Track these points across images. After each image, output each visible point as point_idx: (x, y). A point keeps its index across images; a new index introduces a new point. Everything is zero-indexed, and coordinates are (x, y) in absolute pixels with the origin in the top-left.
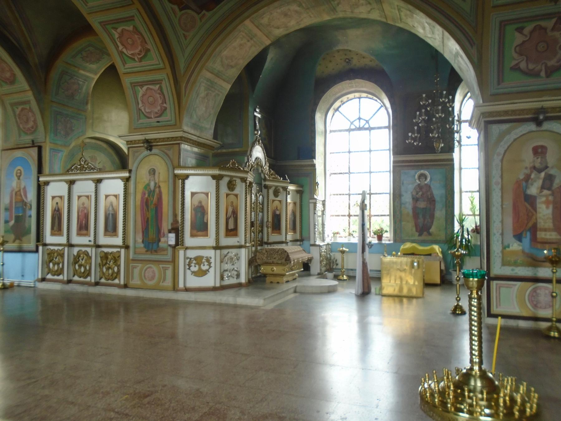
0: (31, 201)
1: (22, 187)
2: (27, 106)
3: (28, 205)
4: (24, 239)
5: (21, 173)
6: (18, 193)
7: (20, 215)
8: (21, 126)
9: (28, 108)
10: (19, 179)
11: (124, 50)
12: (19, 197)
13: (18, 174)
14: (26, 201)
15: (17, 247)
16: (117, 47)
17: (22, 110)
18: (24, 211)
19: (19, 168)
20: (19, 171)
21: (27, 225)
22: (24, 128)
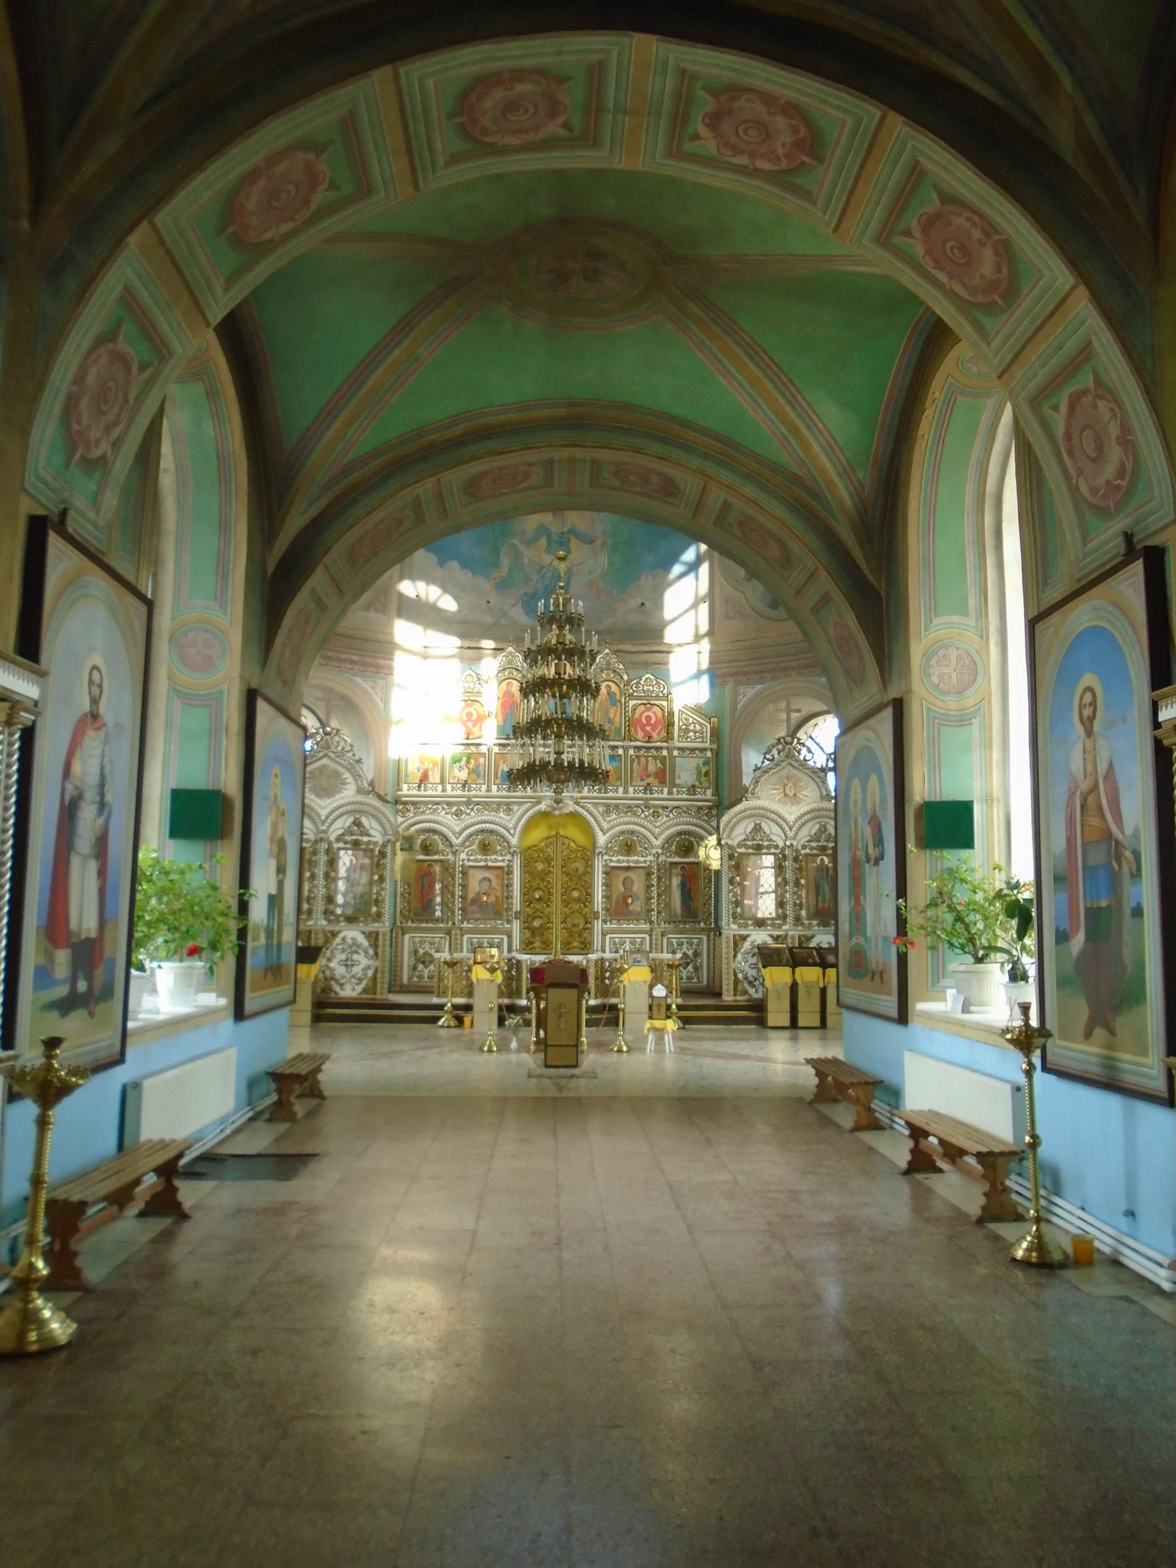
0: (1136, 834)
1: (1102, 768)
3: (1128, 854)
4: (1122, 1023)
5: (1094, 704)
6: (1091, 799)
10: (1089, 733)
12: (1094, 821)
13: (1087, 712)
14: (1120, 837)
15: (1095, 1060)
18: (1115, 885)
19: (1088, 679)
20: (1088, 698)
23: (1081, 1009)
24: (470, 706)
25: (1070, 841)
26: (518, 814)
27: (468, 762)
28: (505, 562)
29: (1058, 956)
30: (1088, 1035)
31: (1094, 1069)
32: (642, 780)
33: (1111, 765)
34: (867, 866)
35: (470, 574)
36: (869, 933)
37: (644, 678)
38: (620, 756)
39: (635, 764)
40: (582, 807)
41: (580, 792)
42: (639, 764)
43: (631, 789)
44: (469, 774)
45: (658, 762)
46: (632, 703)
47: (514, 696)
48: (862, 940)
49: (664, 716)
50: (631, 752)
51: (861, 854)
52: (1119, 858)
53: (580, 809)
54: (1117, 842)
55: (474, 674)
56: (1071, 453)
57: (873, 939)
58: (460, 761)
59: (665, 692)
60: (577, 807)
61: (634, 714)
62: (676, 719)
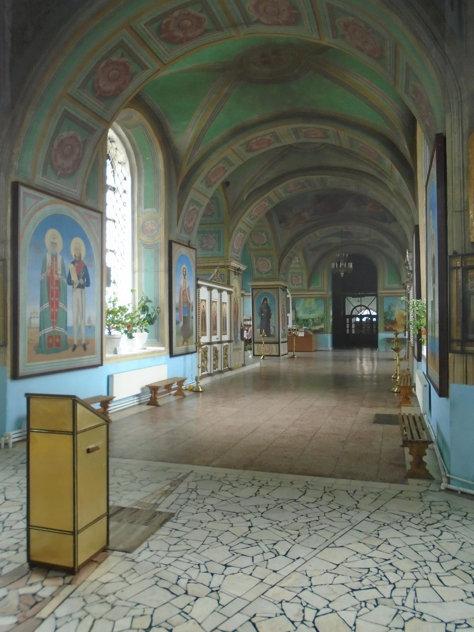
0: (193, 302)
1: (187, 287)
2: (198, 209)
3: (191, 306)
4: (189, 340)
5: (186, 272)
7: (187, 315)
8: (185, 223)
9: (198, 210)
10: (185, 278)
11: (254, 211)
12: (185, 297)
16: (254, 208)
17: (194, 209)
18: (189, 313)
20: (184, 270)
21: (191, 326)
22: (186, 226)
23: (182, 338)
25: (180, 301)
29: (177, 327)
30: (183, 344)
31: (184, 351)
33: (188, 288)
34: (69, 287)
36: (70, 323)
48: (58, 329)
51: (59, 276)
52: (189, 306)
54: (189, 303)
56: (188, 215)
57: (75, 329)
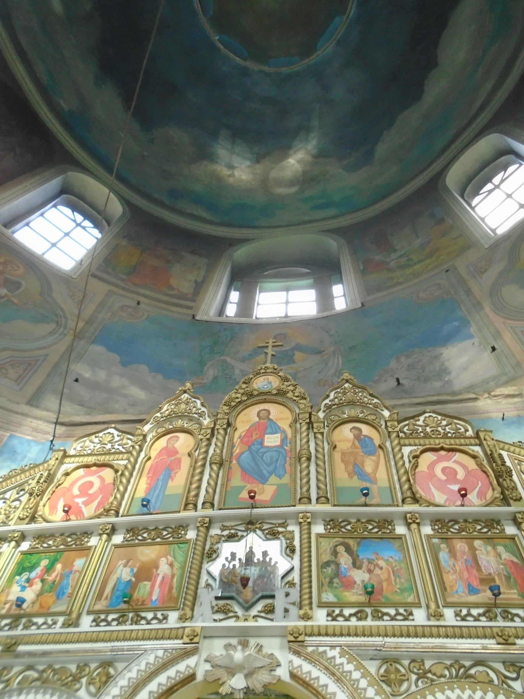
24: (93, 474)
26: (123, 682)
27: (49, 569)
28: (210, 373)
32: (472, 591)
35: (160, 377)
37: (422, 418)
38: (400, 538)
39: (444, 555)
40: (310, 659)
41: (306, 617)
42: (452, 553)
43: (449, 613)
44: (40, 595)
45: (500, 549)
46: (406, 450)
47: (177, 452)
49: (480, 465)
50: (427, 530)
53: (307, 667)
55: (116, 433)
58: (31, 568)
59: (470, 433)
60: (297, 661)
61: (416, 466)
62: (508, 463)
